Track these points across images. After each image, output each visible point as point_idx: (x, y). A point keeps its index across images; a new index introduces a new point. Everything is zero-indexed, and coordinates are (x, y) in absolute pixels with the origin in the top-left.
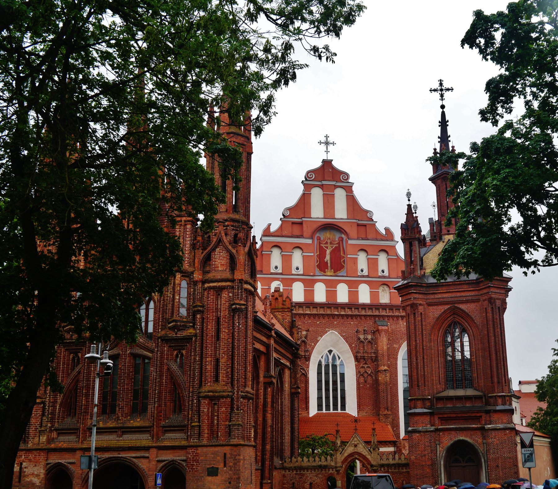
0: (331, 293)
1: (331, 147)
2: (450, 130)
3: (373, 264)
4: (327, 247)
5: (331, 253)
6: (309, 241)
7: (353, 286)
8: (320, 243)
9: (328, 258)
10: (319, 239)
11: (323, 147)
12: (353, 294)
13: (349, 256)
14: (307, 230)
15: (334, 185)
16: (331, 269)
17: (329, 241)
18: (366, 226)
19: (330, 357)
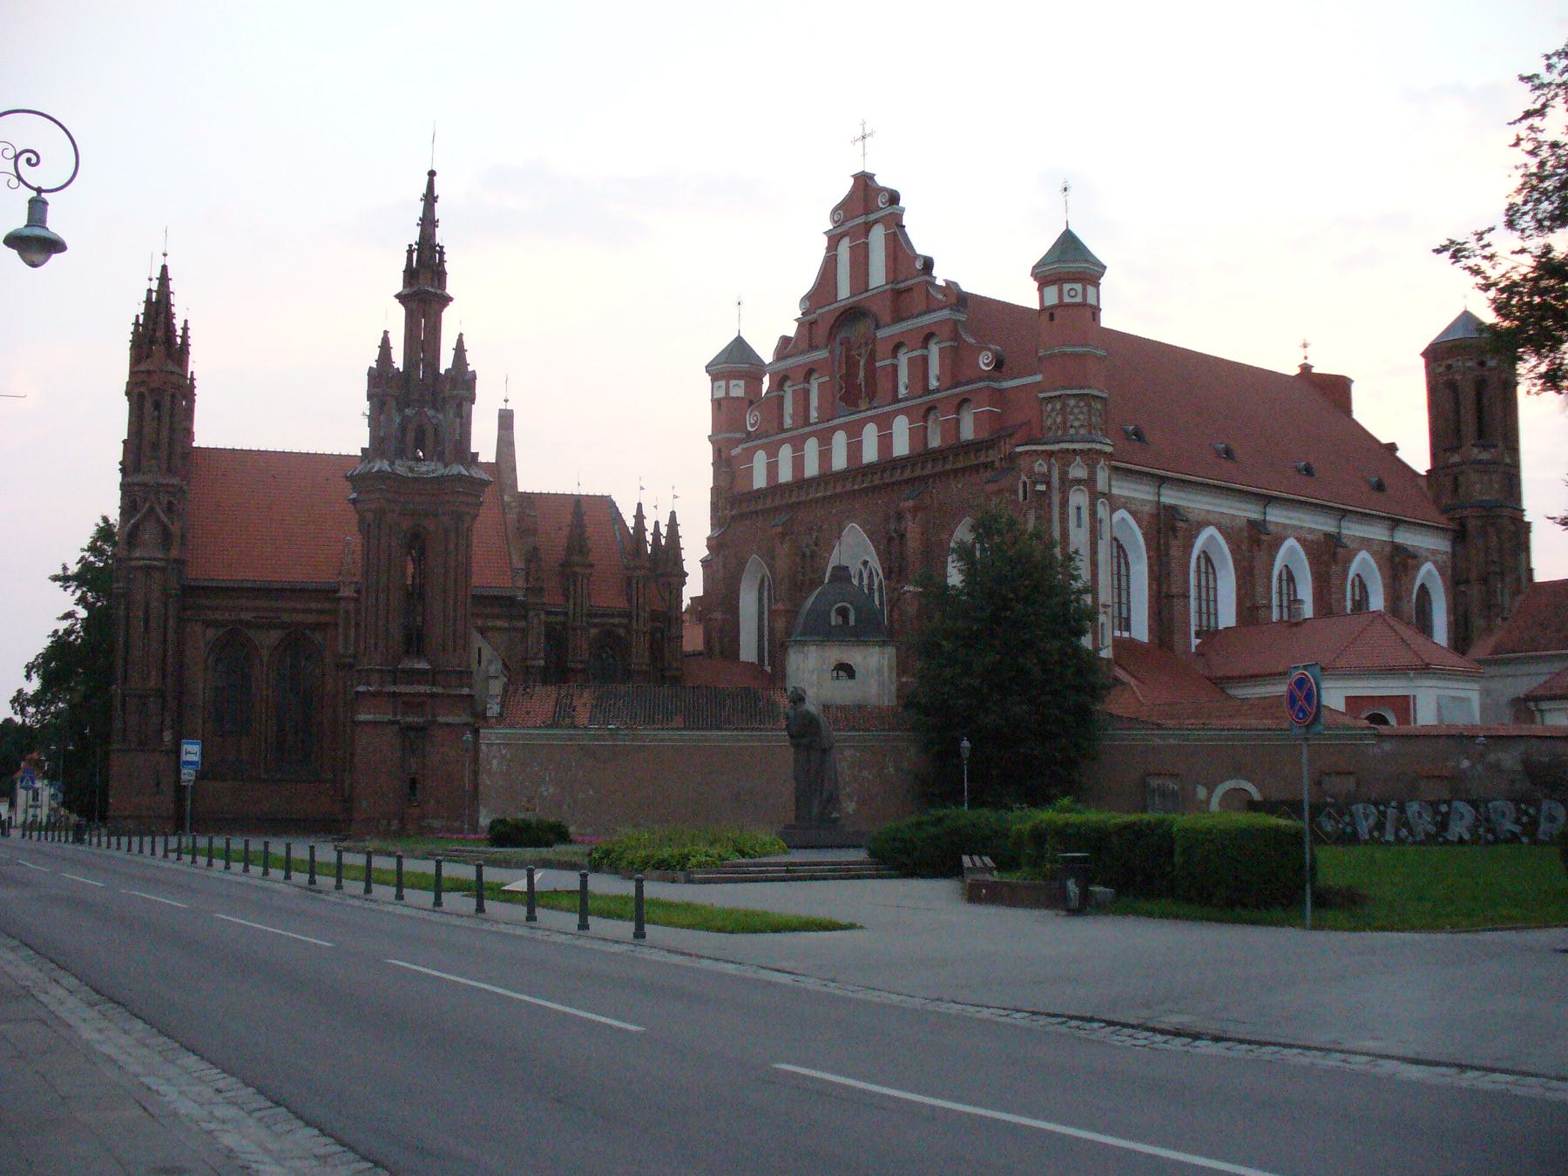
0: (855, 449)
1: (868, 140)
2: (440, 210)
3: (920, 367)
4: (860, 355)
5: (865, 364)
6: (822, 354)
7: (884, 423)
8: (848, 350)
9: (862, 374)
10: (846, 343)
11: (860, 143)
12: (885, 441)
13: (878, 364)
14: (822, 330)
15: (866, 223)
16: (867, 395)
17: (863, 341)
18: (911, 289)
19: (865, 576)
